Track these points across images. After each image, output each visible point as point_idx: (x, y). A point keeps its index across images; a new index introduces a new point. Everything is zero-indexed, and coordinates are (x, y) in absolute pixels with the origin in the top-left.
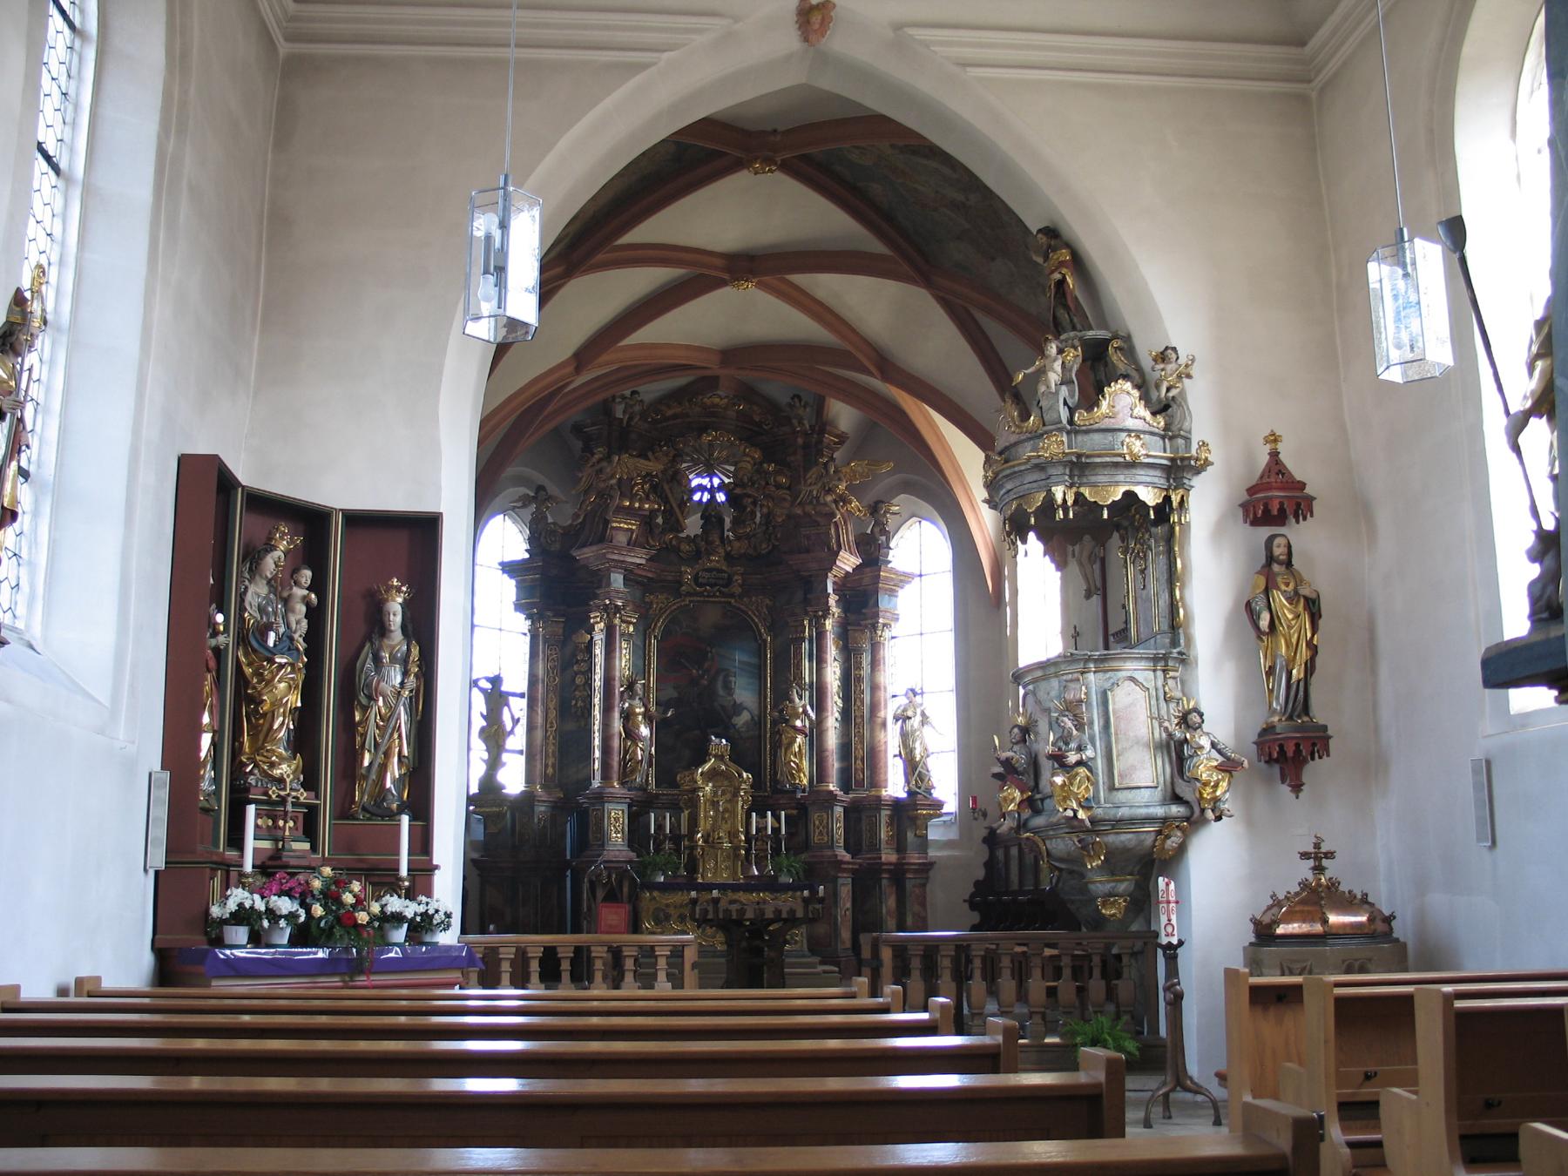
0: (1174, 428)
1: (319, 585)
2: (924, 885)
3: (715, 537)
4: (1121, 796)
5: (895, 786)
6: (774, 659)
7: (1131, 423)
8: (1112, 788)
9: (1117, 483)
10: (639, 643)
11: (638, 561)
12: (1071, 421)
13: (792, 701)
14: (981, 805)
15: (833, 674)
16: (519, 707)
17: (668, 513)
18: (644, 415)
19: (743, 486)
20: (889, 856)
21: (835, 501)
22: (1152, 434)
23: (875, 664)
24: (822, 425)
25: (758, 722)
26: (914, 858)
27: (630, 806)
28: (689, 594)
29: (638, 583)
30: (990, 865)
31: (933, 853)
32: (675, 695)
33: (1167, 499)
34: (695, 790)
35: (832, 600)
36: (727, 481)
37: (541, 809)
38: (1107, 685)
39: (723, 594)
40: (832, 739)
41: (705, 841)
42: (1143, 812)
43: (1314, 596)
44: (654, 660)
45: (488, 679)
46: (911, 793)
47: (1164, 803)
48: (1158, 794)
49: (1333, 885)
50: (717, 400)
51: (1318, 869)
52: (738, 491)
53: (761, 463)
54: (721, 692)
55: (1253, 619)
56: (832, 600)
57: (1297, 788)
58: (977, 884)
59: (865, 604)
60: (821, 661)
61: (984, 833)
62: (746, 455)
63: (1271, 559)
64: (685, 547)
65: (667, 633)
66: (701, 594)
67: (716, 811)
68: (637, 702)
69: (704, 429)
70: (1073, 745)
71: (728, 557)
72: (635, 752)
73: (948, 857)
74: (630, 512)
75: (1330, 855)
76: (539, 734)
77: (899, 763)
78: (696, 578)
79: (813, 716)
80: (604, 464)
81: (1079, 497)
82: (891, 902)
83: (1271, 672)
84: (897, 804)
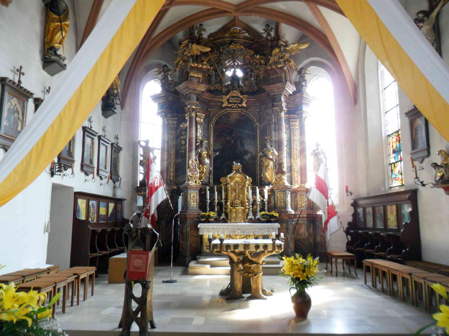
6: (261, 132)
11: (202, 90)
13: (267, 148)
14: (349, 190)
19: (247, 65)
21: (285, 62)
24: (278, 37)
28: (226, 107)
29: (204, 102)
30: (355, 215)
32: (221, 147)
35: (284, 105)
36: (240, 63)
39: (239, 107)
41: (232, 206)
44: (212, 134)
50: (235, 30)
52: (245, 67)
53: (254, 55)
59: (297, 110)
61: (352, 201)
64: (224, 90)
65: (217, 123)
66: (230, 107)
68: (204, 149)
69: (231, 43)
71: (242, 93)
72: (203, 169)
76: (165, 163)
78: (228, 100)
79: (277, 154)
80: (185, 48)
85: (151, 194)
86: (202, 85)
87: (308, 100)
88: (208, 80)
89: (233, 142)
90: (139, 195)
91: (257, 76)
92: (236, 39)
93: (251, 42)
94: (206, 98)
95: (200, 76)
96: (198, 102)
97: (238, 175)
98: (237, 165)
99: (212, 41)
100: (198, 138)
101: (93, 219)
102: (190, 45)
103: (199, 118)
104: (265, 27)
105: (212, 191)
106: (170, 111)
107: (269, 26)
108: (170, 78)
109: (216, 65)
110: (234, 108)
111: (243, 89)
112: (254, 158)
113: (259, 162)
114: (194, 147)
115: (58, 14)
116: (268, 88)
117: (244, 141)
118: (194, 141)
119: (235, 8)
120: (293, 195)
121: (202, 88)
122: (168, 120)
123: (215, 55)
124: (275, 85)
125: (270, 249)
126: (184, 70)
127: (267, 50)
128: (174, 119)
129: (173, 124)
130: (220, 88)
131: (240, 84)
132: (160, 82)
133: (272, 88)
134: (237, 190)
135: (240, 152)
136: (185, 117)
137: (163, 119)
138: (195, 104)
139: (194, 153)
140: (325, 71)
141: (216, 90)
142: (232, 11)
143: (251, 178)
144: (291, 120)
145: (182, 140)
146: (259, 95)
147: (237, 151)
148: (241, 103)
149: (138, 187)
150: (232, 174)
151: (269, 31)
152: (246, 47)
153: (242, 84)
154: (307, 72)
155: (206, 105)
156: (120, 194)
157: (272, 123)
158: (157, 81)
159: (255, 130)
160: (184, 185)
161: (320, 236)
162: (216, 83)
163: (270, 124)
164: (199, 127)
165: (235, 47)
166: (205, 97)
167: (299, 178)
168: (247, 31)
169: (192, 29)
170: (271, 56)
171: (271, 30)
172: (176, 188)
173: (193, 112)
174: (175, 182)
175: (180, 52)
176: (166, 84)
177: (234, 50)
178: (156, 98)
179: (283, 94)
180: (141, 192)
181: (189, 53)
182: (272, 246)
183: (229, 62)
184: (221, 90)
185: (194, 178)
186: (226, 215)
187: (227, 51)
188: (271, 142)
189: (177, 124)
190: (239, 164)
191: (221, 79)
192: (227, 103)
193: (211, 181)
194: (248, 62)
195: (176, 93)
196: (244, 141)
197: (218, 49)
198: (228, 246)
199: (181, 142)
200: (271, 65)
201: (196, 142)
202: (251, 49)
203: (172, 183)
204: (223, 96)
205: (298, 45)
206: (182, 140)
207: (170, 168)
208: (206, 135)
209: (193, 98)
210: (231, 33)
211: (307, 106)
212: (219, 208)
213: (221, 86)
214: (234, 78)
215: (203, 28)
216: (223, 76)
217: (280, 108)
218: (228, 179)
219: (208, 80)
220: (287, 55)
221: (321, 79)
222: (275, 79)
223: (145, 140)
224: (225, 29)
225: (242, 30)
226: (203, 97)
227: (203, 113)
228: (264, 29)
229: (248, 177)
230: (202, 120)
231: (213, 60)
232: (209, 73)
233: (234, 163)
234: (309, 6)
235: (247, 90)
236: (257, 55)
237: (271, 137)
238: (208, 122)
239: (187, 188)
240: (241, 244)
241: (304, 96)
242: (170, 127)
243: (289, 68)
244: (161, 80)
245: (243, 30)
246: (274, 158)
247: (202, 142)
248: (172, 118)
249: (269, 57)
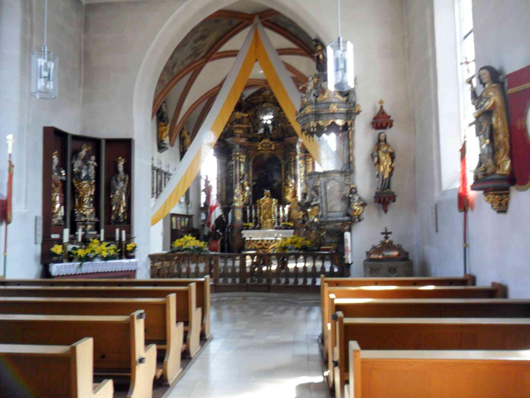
0: (350, 100)
1: (98, 160)
3: (267, 133)
4: (330, 214)
7: (334, 100)
8: (327, 212)
9: (329, 120)
12: (316, 101)
17: (254, 127)
18: (246, 100)
22: (341, 103)
28: (260, 150)
33: (346, 124)
38: (326, 181)
42: (335, 219)
43: (392, 151)
47: (343, 216)
48: (342, 214)
49: (391, 242)
51: (387, 238)
54: (269, 176)
55: (375, 159)
57: (386, 211)
60: (295, 167)
63: (379, 141)
64: (259, 137)
65: (254, 161)
69: (264, 102)
70: (315, 199)
71: (271, 139)
74: (240, 128)
75: (390, 233)
76: (219, 190)
81: (318, 124)
83: (378, 175)
85: (211, 212)
97: (267, 199)
101: (179, 228)
105: (251, 209)
112: (280, 185)
114: (238, 180)
115: (164, 122)
118: (238, 176)
125: (274, 242)
139: (238, 184)
155: (245, 149)
156: (191, 212)
159: (280, 165)
162: (253, 133)
163: (290, 162)
185: (238, 202)
186: (260, 225)
193: (251, 202)
198: (254, 241)
210: (264, 96)
227: (245, 155)
239: (234, 208)
247: (244, 175)
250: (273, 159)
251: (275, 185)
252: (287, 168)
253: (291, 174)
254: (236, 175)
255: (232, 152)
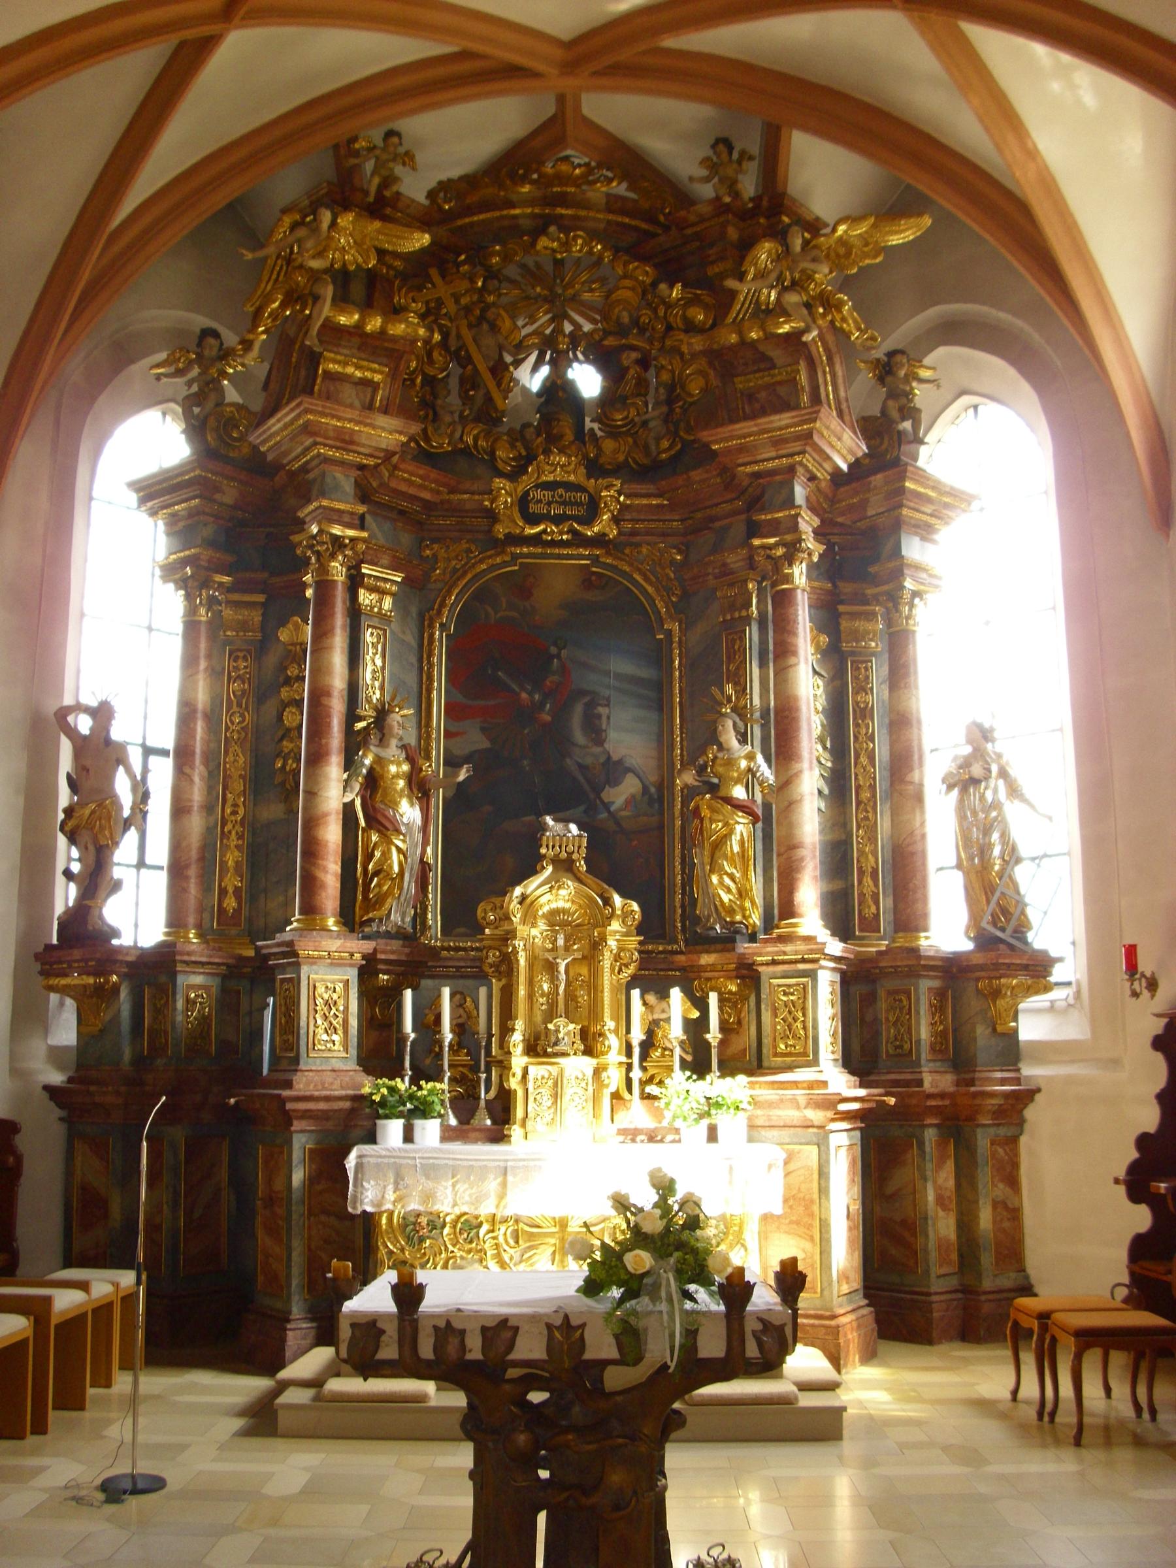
2: (1014, 1141)
5: (947, 929)
6: (690, 666)
10: (411, 639)
13: (721, 747)
14: (1145, 965)
15: (808, 687)
16: (161, 776)
17: (470, 382)
20: (935, 1079)
21: (808, 306)
23: (899, 673)
25: (657, 796)
26: (996, 1083)
27: (367, 970)
29: (402, 513)
31: (1030, 1071)
32: (485, 744)
34: (511, 935)
35: (807, 524)
36: (587, 327)
37: (194, 984)
39: (579, 540)
40: (810, 823)
45: (93, 712)
46: (984, 941)
50: (564, 168)
52: (610, 342)
53: (654, 285)
54: (579, 737)
56: (807, 524)
58: (1143, 1141)
59: (876, 559)
60: (780, 653)
61: (1158, 1026)
62: (625, 277)
66: (536, 540)
67: (554, 979)
68: (393, 750)
71: (595, 468)
72: (386, 855)
73: (1069, 1080)
76: (196, 824)
77: (957, 880)
78: (523, 502)
80: (302, 232)
82: (946, 1177)
84: (952, 969)
86: (382, 420)
87: (928, 509)
88: (421, 400)
89: (549, 718)
90: (52, 989)
91: (673, 391)
92: (570, 212)
93: (644, 226)
94: (412, 491)
95: (377, 378)
96: (361, 509)
98: (563, 833)
99: (450, 216)
100: (362, 696)
102: (326, 216)
103: (372, 589)
104: (710, 153)
106: (229, 558)
107: (730, 149)
108: (232, 395)
109: (467, 335)
110: (553, 543)
111: (599, 449)
113: (678, 823)
116: (721, 438)
117: (601, 710)
118: (337, 707)
119: (559, 53)
120: (857, 990)
121: (386, 433)
122: (211, 602)
123: (465, 285)
124: (762, 421)
126: (292, 342)
127: (722, 259)
128: (247, 598)
129: (243, 626)
130: (482, 443)
131: (588, 424)
132: (179, 410)
133: (751, 440)
134: (562, 968)
135: (582, 767)
136: (304, 586)
137: (189, 597)
138: (346, 519)
139: (334, 771)
140: (1012, 372)
141: (466, 452)
142: (540, 67)
143: (635, 906)
144: (841, 608)
145: (285, 705)
146: (680, 481)
147: (568, 761)
148: (589, 521)
149: (49, 947)
150: (532, 885)
151: (730, 171)
152: (617, 251)
153: (596, 426)
154: (925, 374)
157: (747, 620)
158: (174, 413)
159: (659, 657)
160: (279, 938)
161: (995, 1204)
163: (735, 627)
164: (369, 637)
165: (566, 246)
166: (403, 488)
167: (890, 902)
168: (625, 176)
169: (344, 151)
170: (741, 277)
171: (739, 162)
172: (251, 953)
173: (333, 556)
174: (250, 920)
175: (271, 250)
176: (212, 422)
177: (559, 264)
178: (155, 492)
179: (800, 470)
180: (65, 975)
181: (320, 254)
182: (721, 1329)
183: (532, 319)
184: (492, 453)
187: (523, 266)
188: (742, 716)
189: (263, 628)
190: (574, 828)
191: (489, 399)
192: (517, 516)
193: (434, 919)
194: (626, 318)
195: (258, 466)
196: (601, 710)
197: (478, 254)
199: (280, 718)
200: (738, 326)
201: (352, 716)
202: (644, 259)
203: (234, 931)
204: (499, 482)
205: (874, 226)
206: (285, 705)
207: (225, 848)
208: (411, 679)
209: (337, 487)
210: (545, 182)
211: (923, 539)
212: (463, 1058)
213: (488, 434)
214: (558, 392)
215: (401, 150)
216: (499, 385)
217: (789, 538)
218: (514, 906)
219: (424, 404)
220: (823, 274)
221: (989, 409)
222: (763, 395)
223: (94, 703)
224: (513, 163)
225: (600, 166)
226: (393, 484)
228: (705, 161)
229: (618, 900)
230: (387, 603)
231: (450, 307)
232: (431, 371)
233: (549, 820)
234: (924, 29)
235: (621, 458)
236: (671, 287)
237: (742, 690)
238: (421, 616)
240: (533, 1318)
241: (908, 484)
242: (228, 641)
243: (830, 338)
244: (188, 404)
245: (600, 166)
246: (758, 797)
247: (382, 713)
248: (236, 597)
249: (731, 283)
250: (608, 606)
251: (622, 794)
252: (717, 665)
253: (741, 712)
254: (319, 695)
255: (301, 525)
